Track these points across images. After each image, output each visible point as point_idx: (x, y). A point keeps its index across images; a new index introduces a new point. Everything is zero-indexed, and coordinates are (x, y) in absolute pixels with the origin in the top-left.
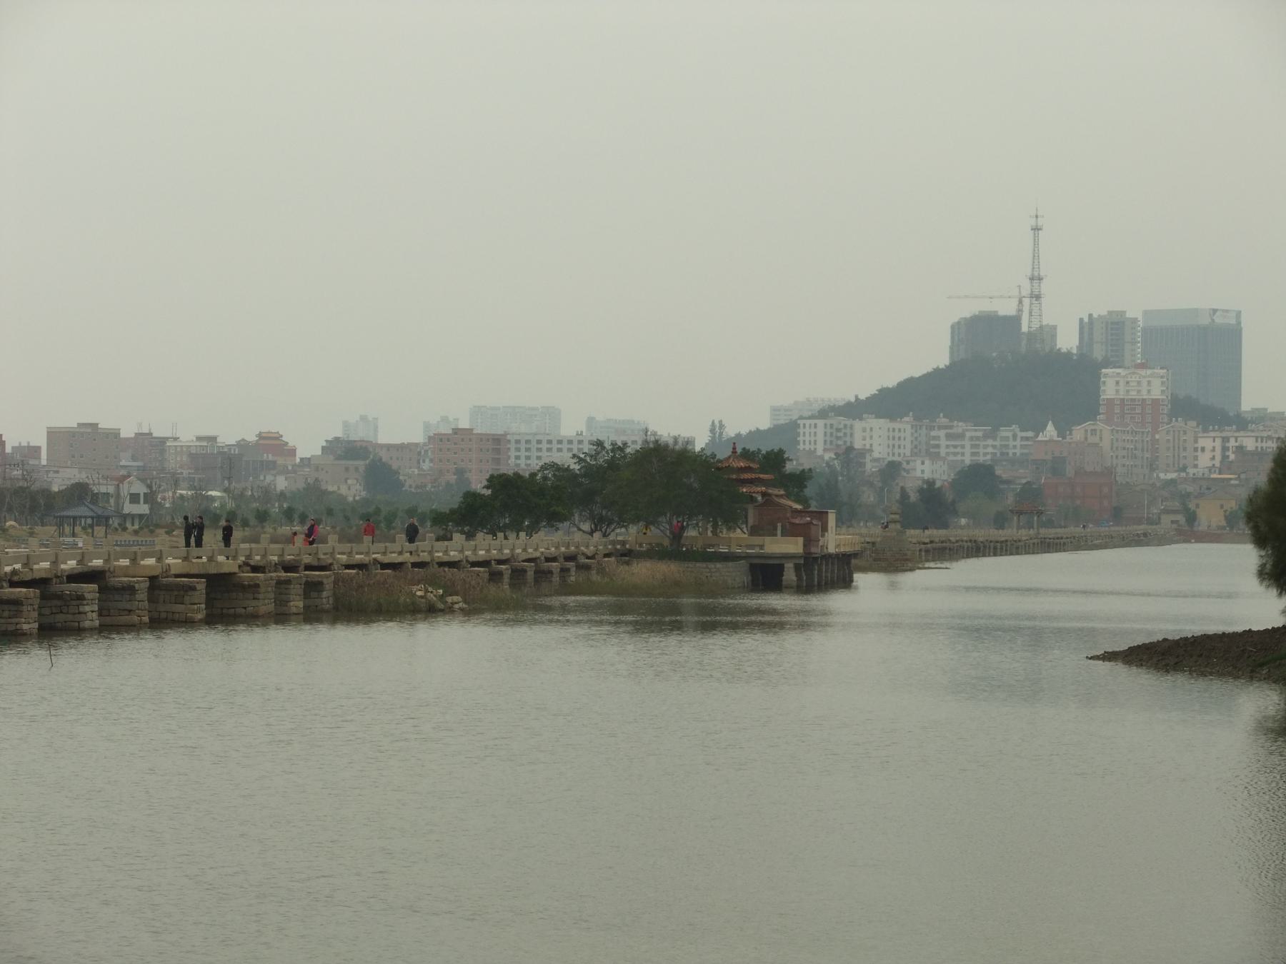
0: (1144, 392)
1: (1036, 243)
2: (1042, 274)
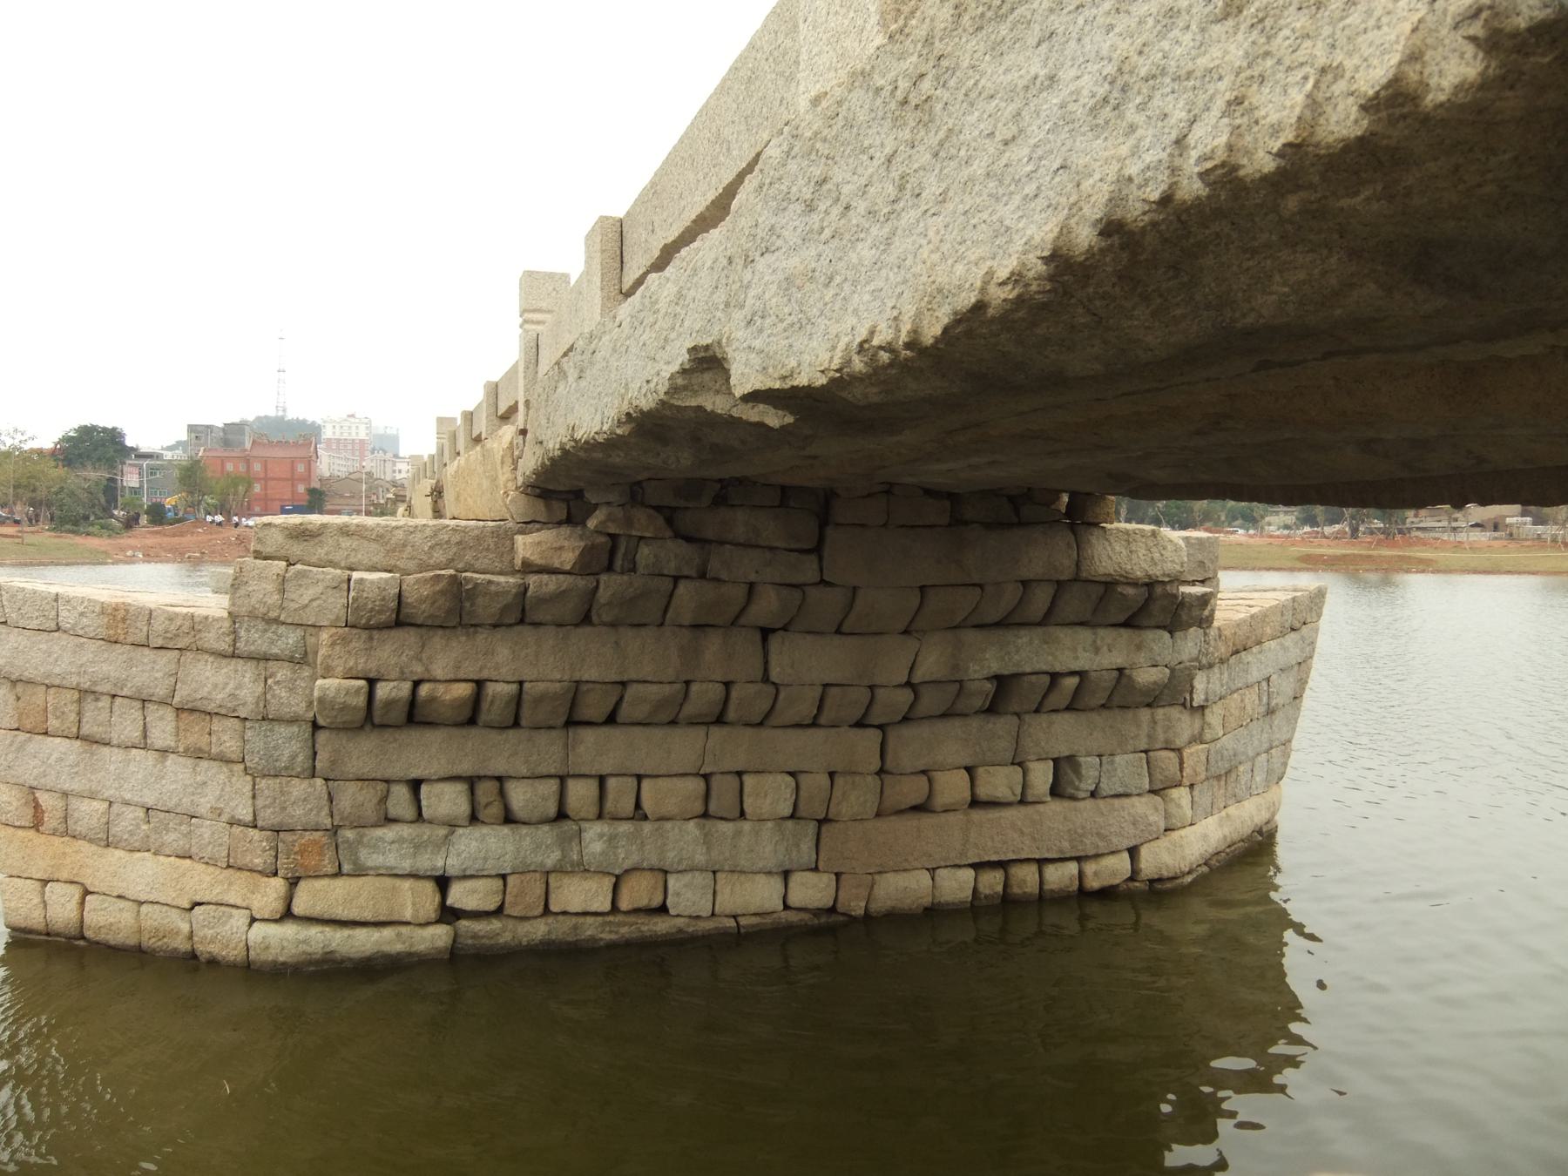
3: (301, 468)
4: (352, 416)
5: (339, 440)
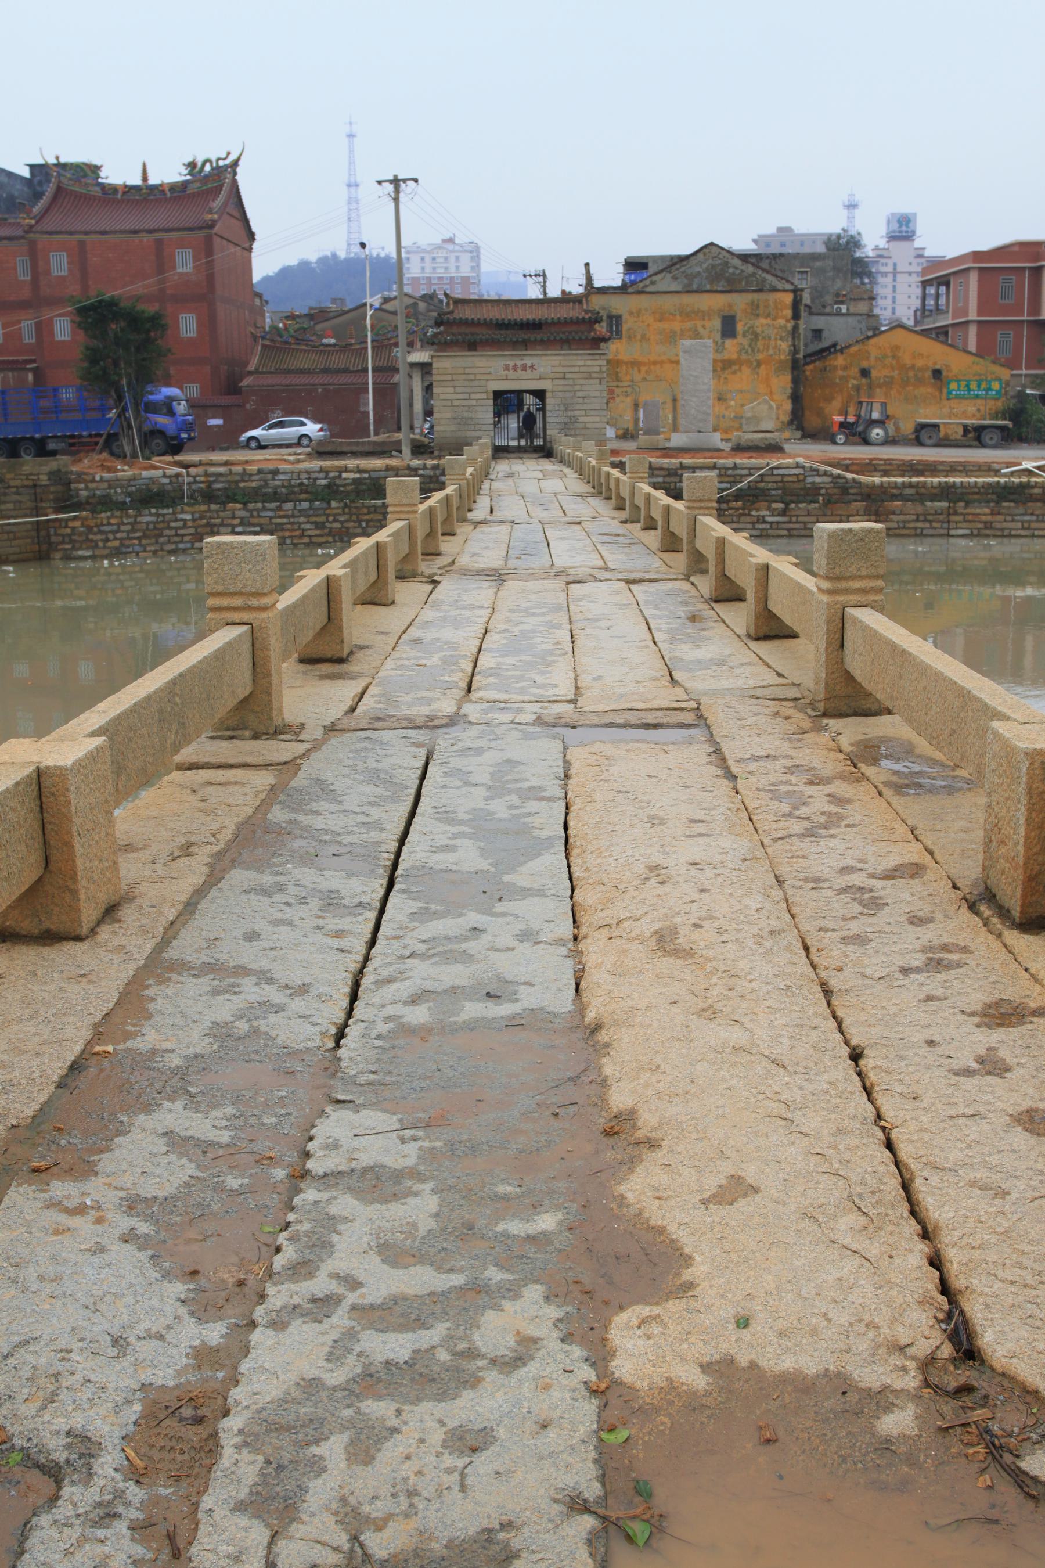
0: (453, 269)
1: (351, 151)
2: (359, 180)
3: (185, 263)
4: (451, 241)
5: (429, 279)
